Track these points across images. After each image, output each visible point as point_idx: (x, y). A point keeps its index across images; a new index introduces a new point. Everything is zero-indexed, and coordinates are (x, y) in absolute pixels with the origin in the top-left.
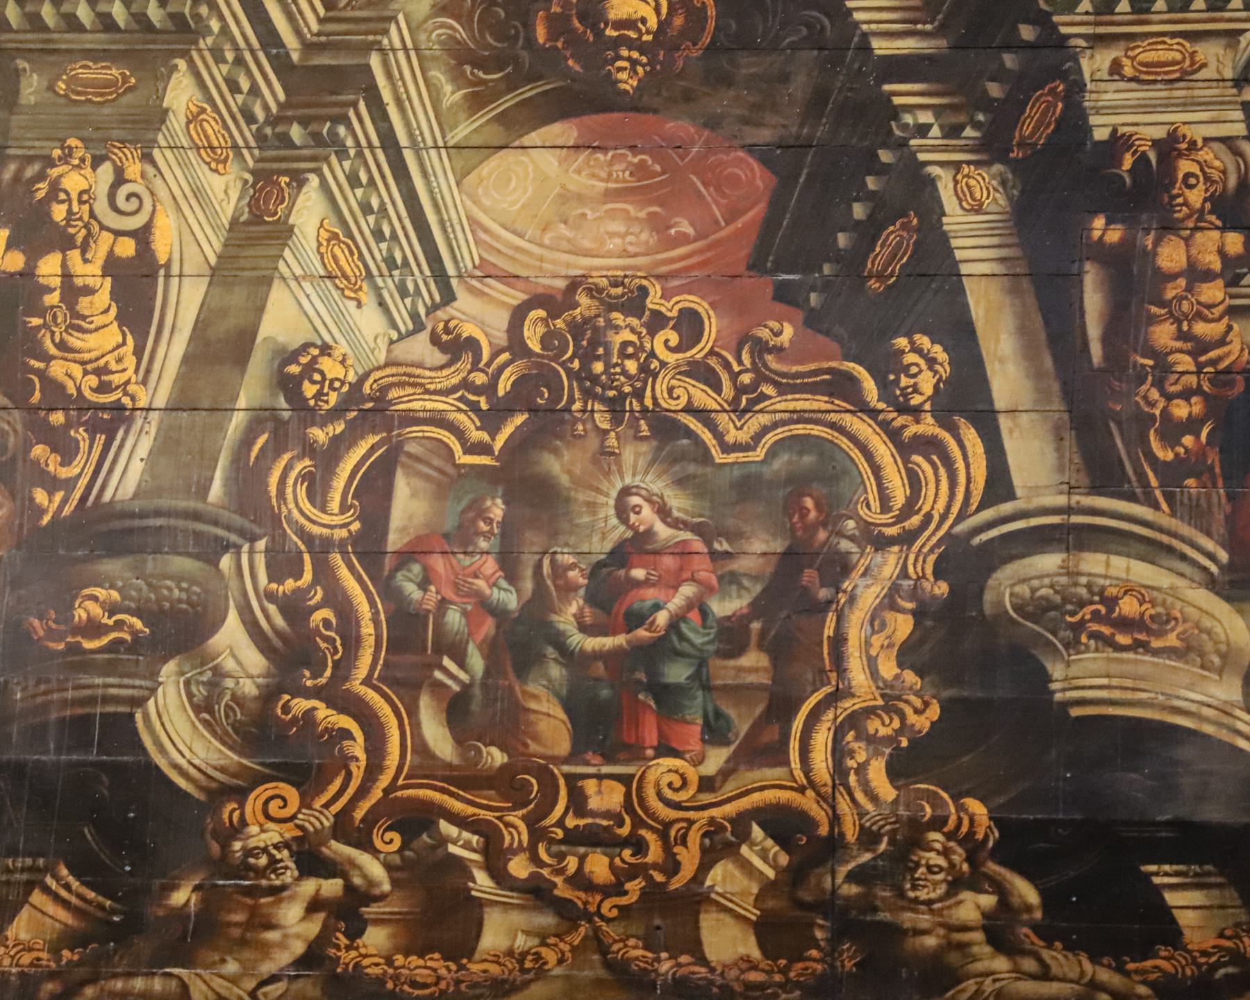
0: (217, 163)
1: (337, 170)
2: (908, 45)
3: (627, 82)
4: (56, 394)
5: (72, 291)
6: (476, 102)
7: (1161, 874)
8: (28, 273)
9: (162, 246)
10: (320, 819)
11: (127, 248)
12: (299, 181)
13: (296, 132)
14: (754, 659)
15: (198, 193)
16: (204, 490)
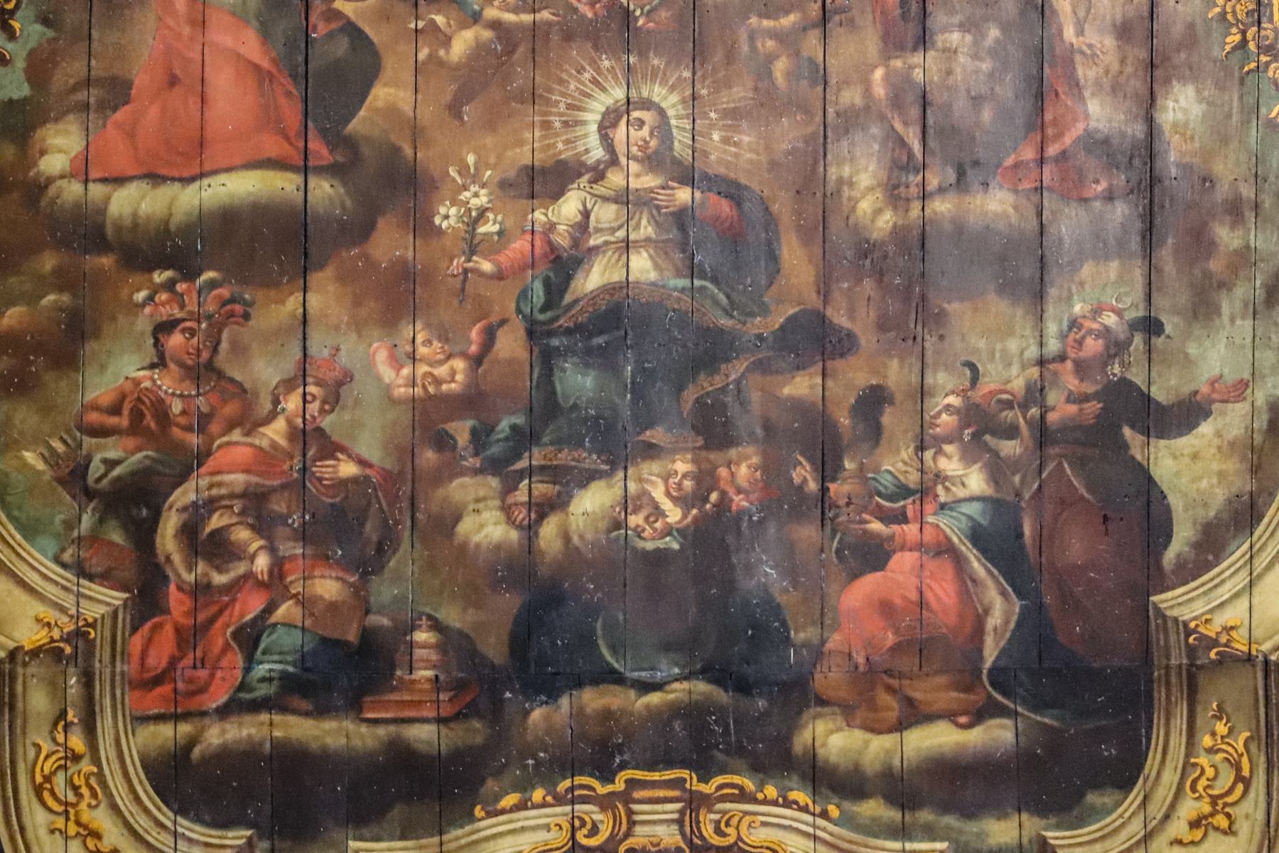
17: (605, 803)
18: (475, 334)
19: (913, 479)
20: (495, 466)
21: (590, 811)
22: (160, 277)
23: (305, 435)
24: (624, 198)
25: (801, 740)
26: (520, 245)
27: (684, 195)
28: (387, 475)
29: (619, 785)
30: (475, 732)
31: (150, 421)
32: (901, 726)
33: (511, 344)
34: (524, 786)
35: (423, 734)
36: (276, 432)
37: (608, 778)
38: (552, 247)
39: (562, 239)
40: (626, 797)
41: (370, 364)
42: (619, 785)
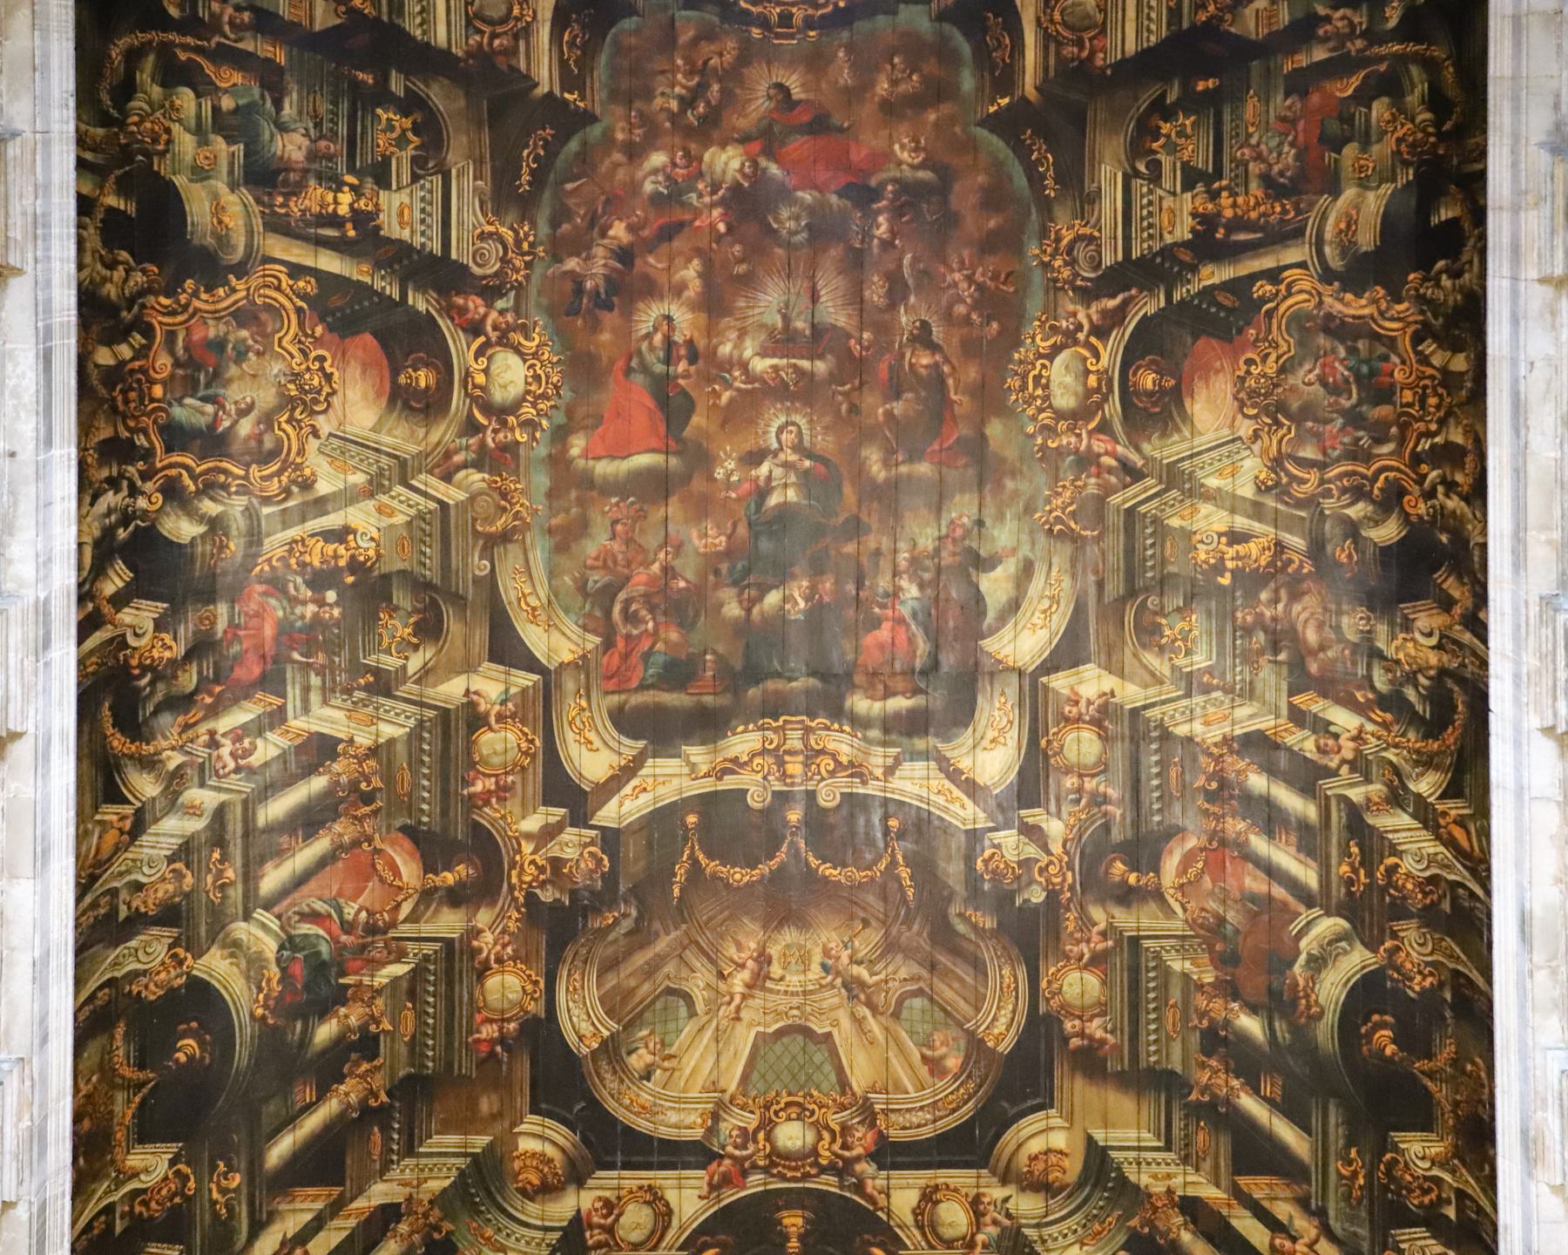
0: (1197, 511)
1: (1199, 474)
2: (1162, 297)
3: (1173, 382)
4: (1271, 564)
5: (1238, 557)
6: (1179, 430)
7: (1434, 220)
8: (1232, 571)
9: (1223, 528)
10: (1416, 489)
11: (1224, 540)
12: (1202, 485)
13: (1187, 486)
14: (1361, 345)
15: (1207, 517)
16: (1303, 518)
17: (775, 730)
18: (729, 525)
19: (891, 590)
20: (735, 583)
21: (769, 734)
22: (614, 500)
23: (668, 571)
24: (786, 465)
25: (848, 704)
26: (746, 486)
27: (807, 463)
28: (695, 586)
29: (781, 723)
30: (724, 700)
31: (610, 563)
32: (885, 697)
33: (742, 530)
34: (746, 724)
35: (708, 700)
36: (656, 567)
37: (776, 720)
38: (758, 486)
39: (762, 483)
40: (783, 728)
41: (690, 541)
42: (781, 723)
